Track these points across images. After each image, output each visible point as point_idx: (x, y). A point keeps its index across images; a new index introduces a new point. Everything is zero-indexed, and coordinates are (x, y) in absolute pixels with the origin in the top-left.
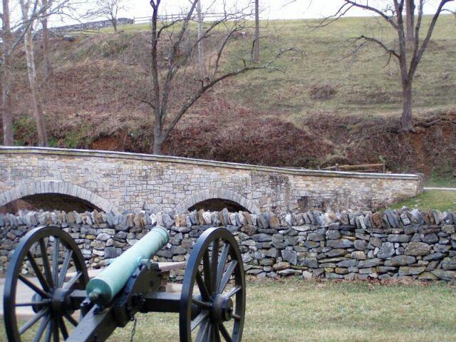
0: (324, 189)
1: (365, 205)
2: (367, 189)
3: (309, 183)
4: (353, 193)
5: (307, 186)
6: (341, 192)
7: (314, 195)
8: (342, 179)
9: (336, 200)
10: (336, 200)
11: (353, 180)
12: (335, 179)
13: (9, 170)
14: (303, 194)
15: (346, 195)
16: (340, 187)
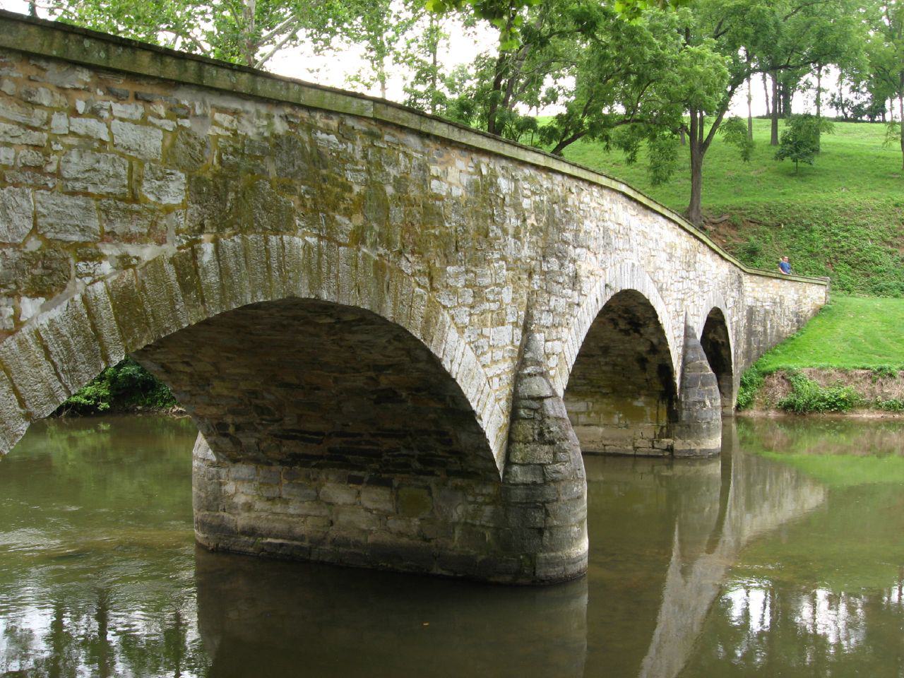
0: (765, 296)
1: (795, 319)
2: (796, 297)
3: (755, 285)
4: (786, 304)
5: (753, 290)
6: (778, 300)
7: (759, 304)
8: (779, 281)
9: (774, 311)
10: (774, 311)
11: (786, 282)
12: (774, 280)
13: (602, 229)
14: (749, 301)
15: (781, 303)
16: (777, 294)
